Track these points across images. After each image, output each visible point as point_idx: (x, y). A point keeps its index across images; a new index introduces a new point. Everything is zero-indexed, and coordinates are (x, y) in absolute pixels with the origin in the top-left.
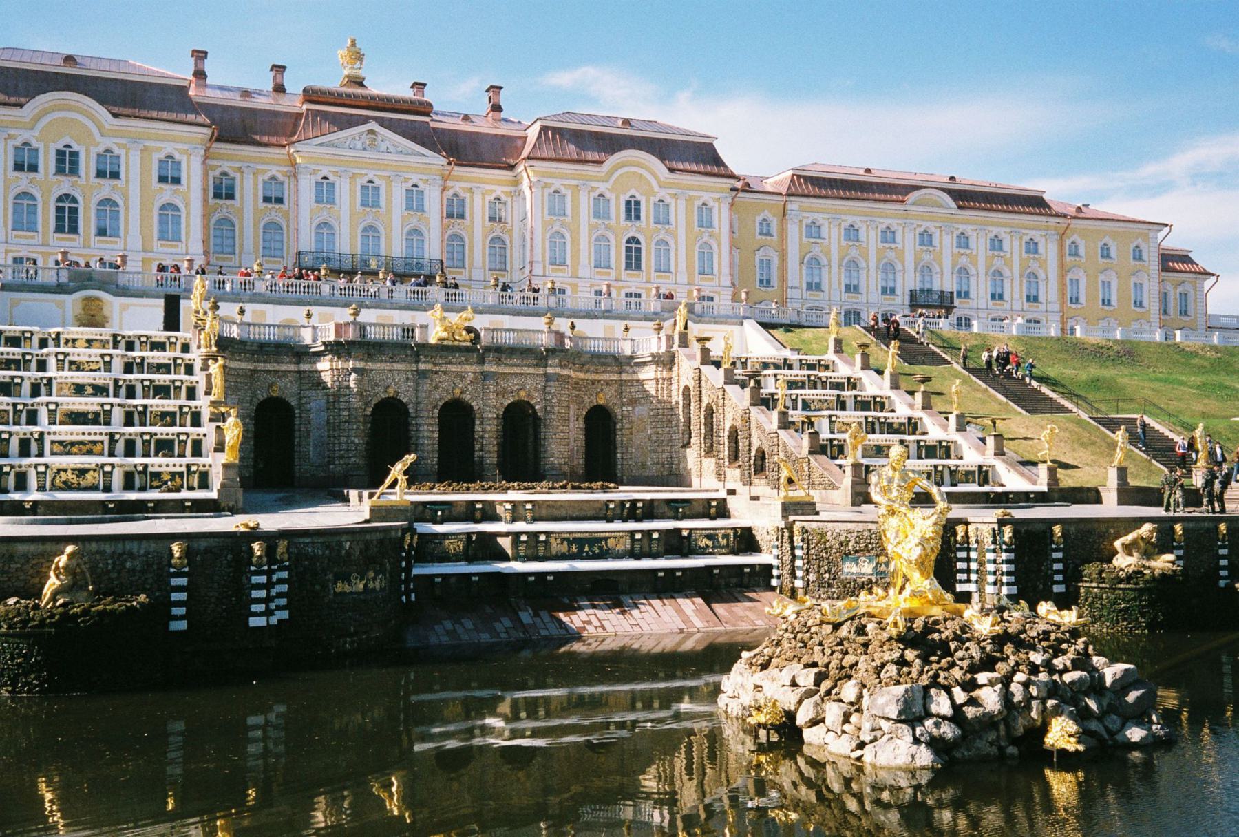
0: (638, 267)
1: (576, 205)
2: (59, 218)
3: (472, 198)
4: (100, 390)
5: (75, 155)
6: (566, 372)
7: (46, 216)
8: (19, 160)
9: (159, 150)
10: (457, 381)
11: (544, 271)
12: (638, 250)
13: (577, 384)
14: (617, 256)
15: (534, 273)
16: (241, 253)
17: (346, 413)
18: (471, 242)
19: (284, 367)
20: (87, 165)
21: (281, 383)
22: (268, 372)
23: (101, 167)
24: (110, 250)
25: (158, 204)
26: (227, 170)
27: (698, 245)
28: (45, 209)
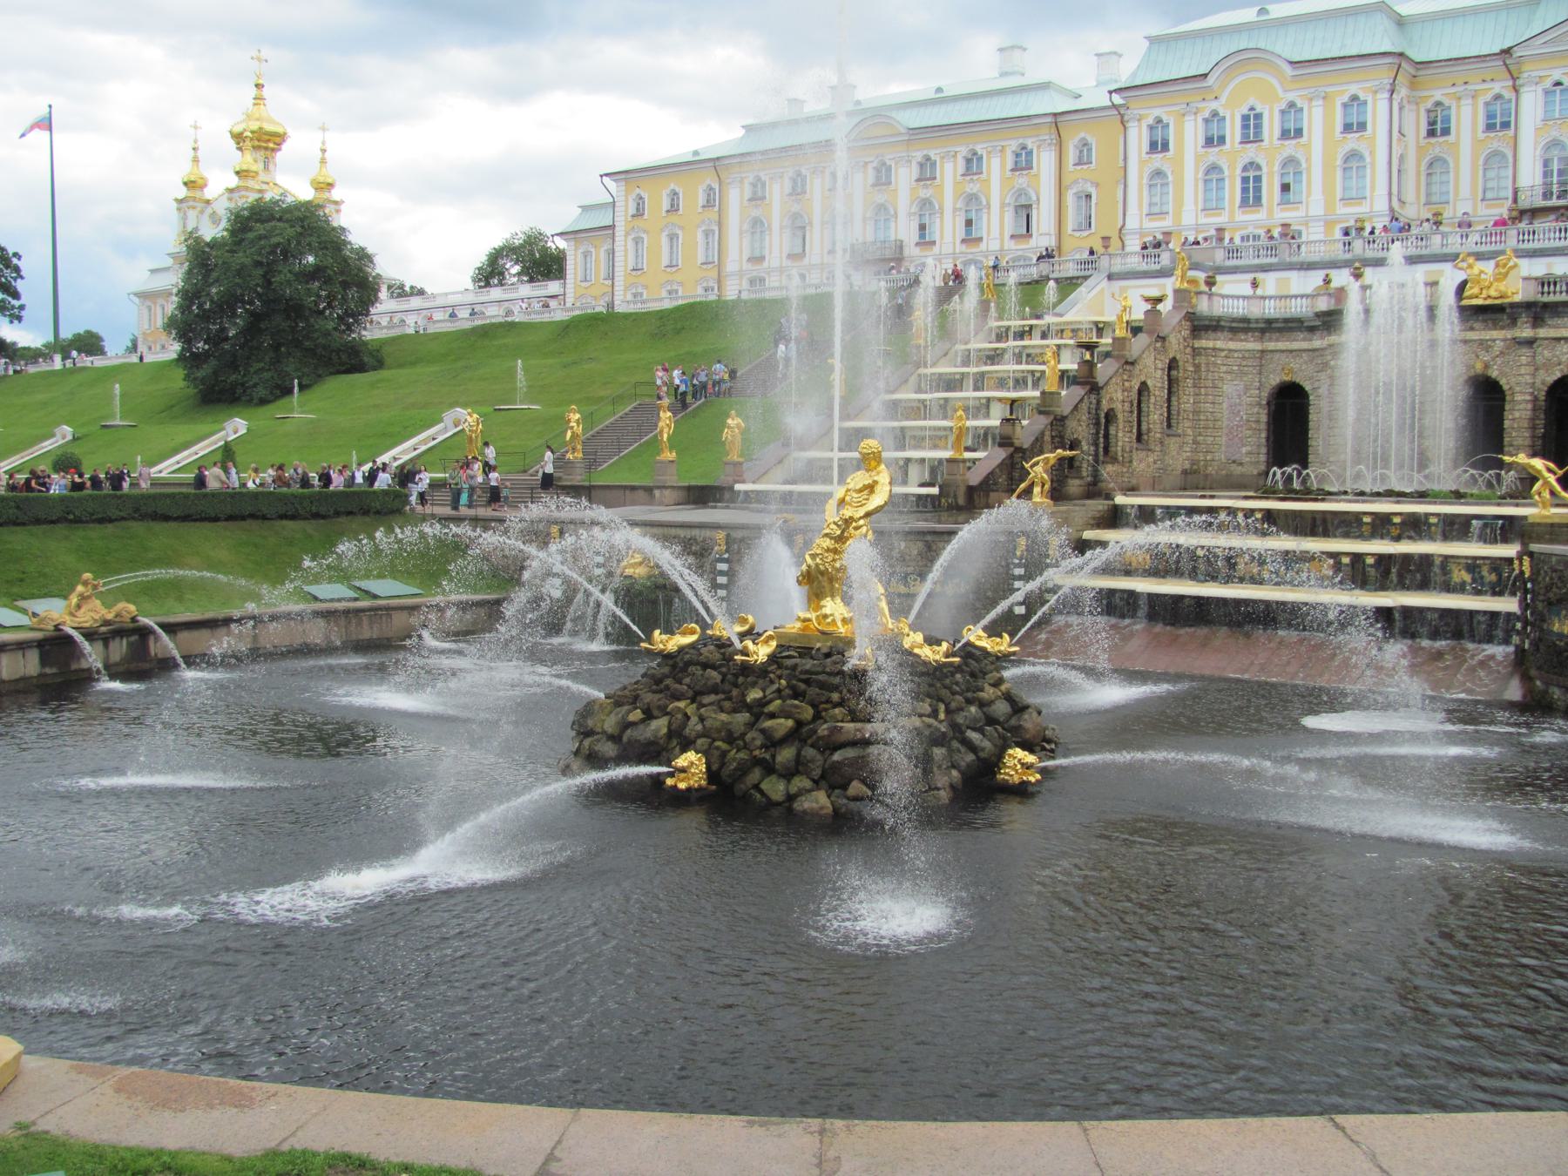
2: (1245, 190)
5: (1258, 117)
7: (1232, 190)
8: (1210, 134)
9: (1343, 92)
10: (1482, 353)
16: (1455, 200)
19: (1295, 345)
20: (1271, 127)
21: (1295, 364)
22: (1282, 351)
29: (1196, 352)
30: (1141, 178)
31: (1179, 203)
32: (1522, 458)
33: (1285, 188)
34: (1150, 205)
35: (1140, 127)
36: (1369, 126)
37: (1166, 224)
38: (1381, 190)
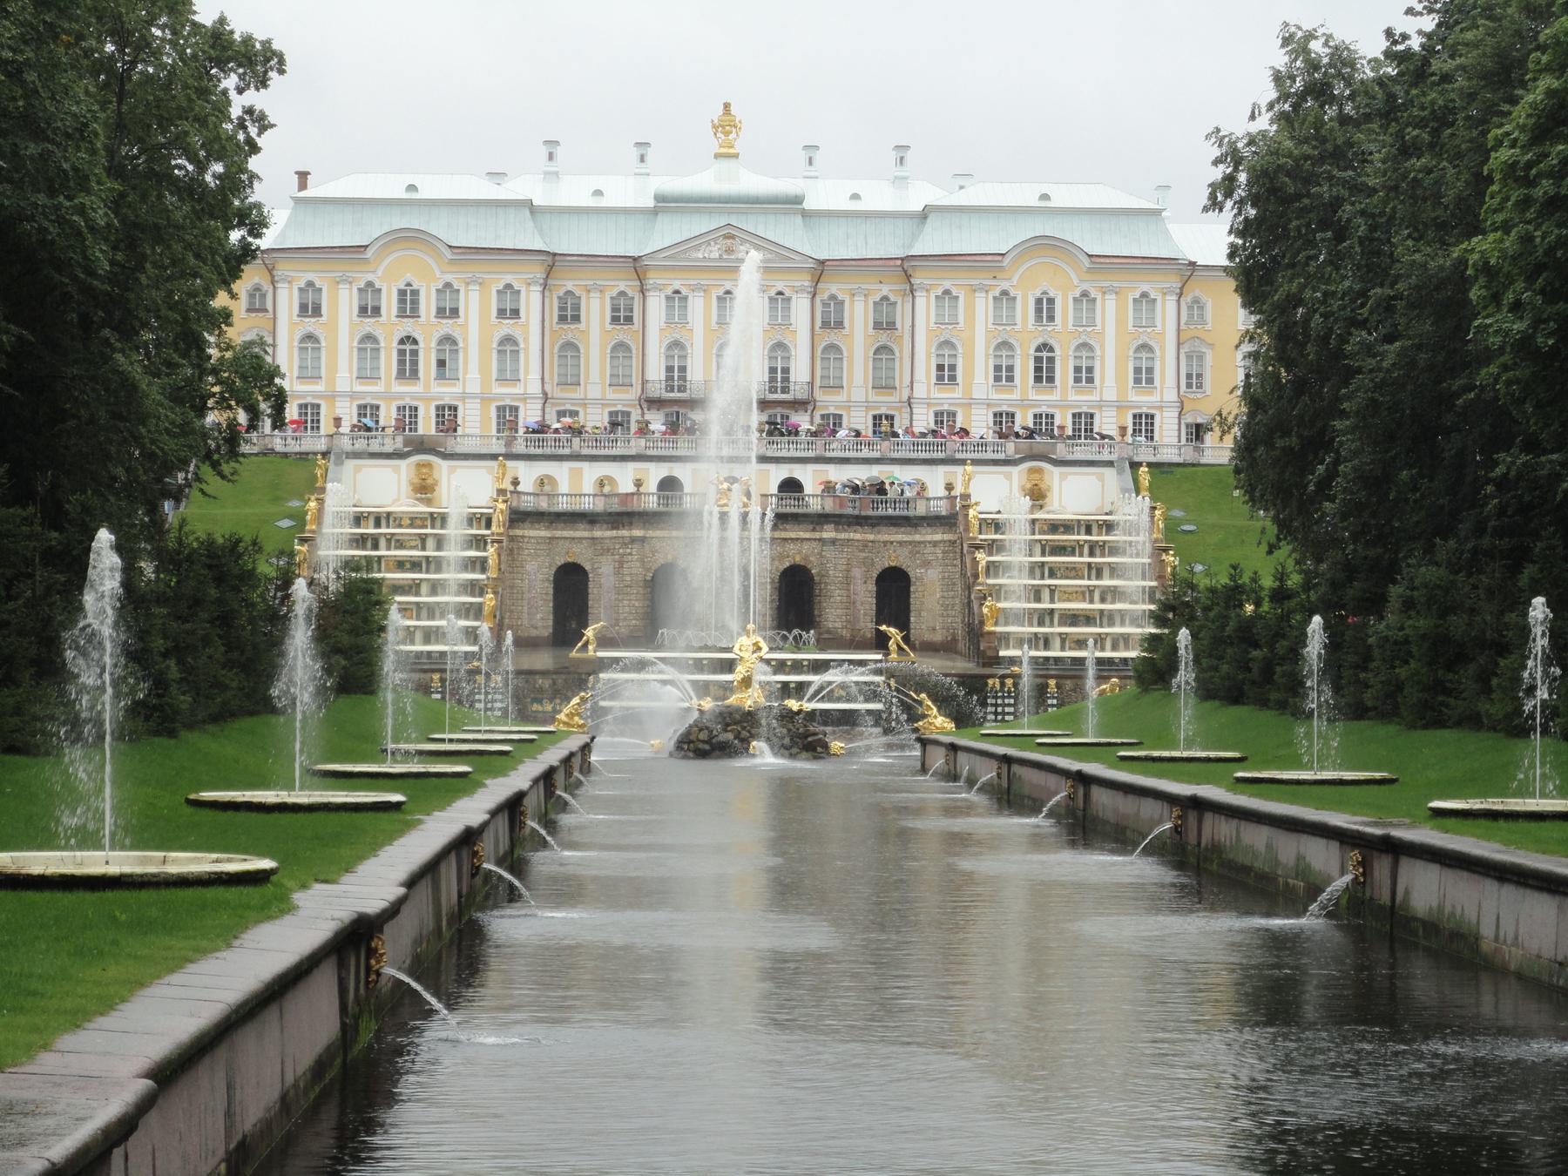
0: (1051, 379)
1: (971, 309)
2: (401, 362)
3: (852, 302)
4: (415, 565)
5: (415, 293)
6: (843, 536)
7: (388, 361)
8: (363, 303)
11: (929, 391)
12: (1051, 360)
13: (865, 545)
14: (1024, 369)
15: (915, 395)
17: (628, 578)
18: (851, 358)
19: (578, 534)
20: (428, 304)
22: (566, 538)
23: (442, 305)
24: (446, 392)
25: (496, 340)
26: (570, 288)
27: (1131, 353)
28: (389, 357)
29: (512, 539)
30: (291, 340)
31: (333, 369)
32: (883, 628)
33: (441, 364)
34: (300, 367)
35: (291, 289)
36: (522, 313)
37: (319, 387)
38: (534, 375)
